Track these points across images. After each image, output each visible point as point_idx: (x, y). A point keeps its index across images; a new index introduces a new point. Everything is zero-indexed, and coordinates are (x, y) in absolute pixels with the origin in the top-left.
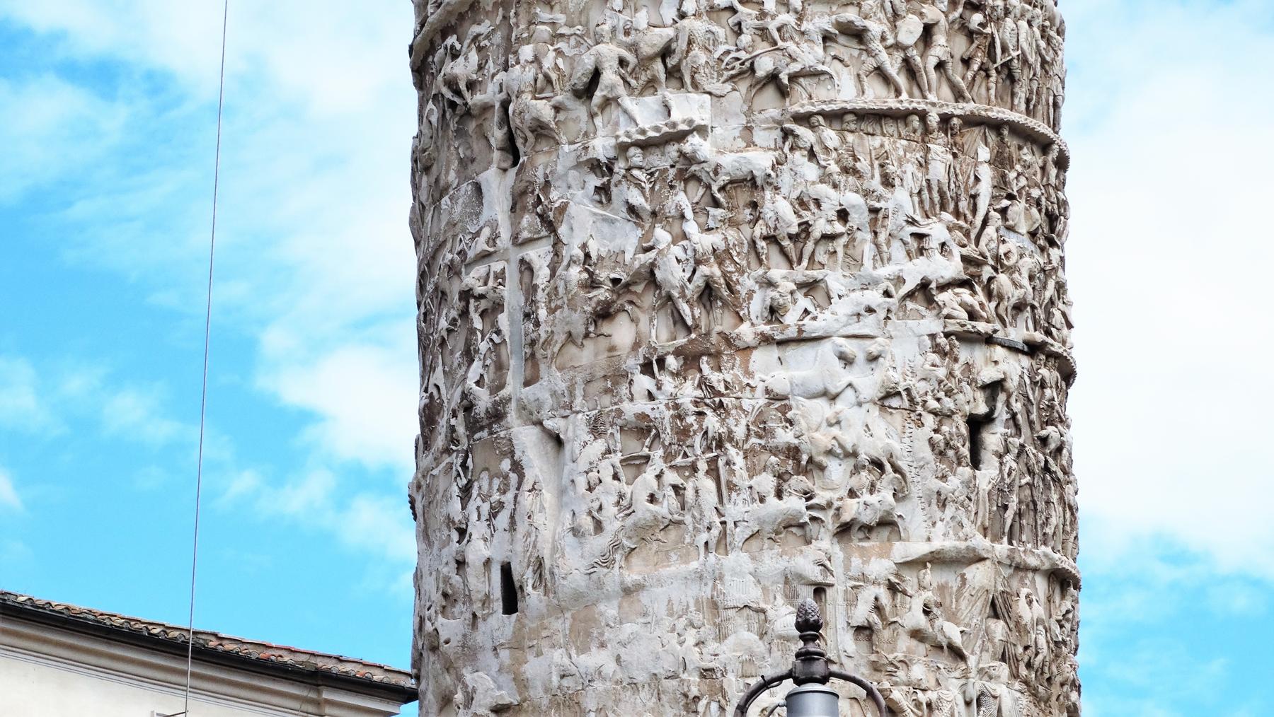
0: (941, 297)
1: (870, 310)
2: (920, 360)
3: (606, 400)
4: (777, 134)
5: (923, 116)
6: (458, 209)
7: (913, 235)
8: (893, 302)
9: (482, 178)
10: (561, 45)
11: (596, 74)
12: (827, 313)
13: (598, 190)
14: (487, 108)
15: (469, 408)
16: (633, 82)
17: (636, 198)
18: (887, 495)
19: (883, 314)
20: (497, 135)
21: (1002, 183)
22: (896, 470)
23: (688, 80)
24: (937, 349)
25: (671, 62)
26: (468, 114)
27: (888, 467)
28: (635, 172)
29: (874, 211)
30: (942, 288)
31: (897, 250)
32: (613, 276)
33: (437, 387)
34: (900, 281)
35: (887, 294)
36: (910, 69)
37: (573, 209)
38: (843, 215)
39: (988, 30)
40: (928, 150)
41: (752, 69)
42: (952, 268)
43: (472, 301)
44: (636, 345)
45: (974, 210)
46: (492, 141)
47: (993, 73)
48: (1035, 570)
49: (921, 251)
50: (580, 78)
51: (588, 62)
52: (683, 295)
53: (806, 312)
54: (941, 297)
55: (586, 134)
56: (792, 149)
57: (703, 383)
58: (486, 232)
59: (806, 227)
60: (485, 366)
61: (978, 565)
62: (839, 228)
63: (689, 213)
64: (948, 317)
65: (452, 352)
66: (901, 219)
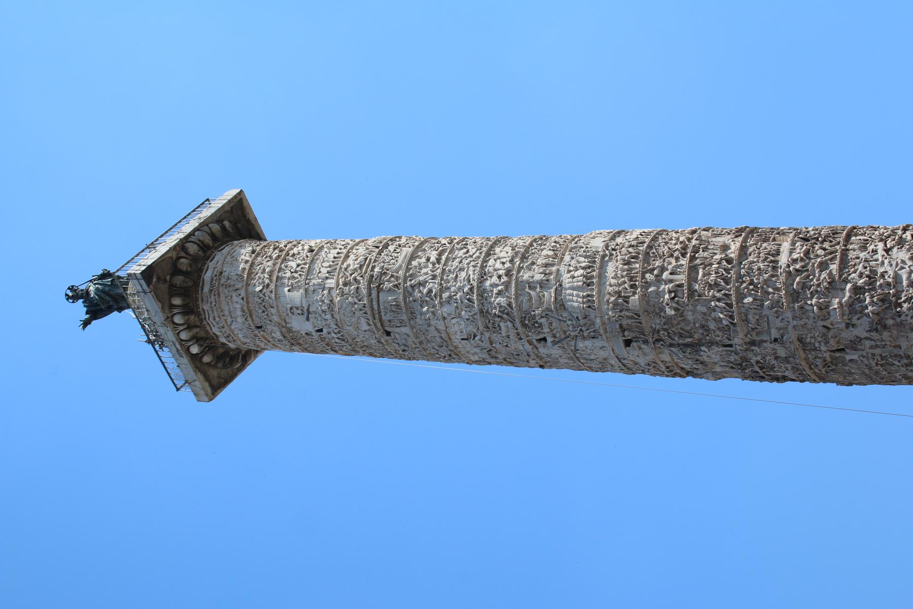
0: (888, 246)
1: (890, 262)
2: (904, 252)
3: (907, 327)
4: (843, 283)
5: (843, 250)
6: (854, 366)
7: (872, 253)
8: (888, 257)
9: (848, 360)
10: (816, 335)
11: (824, 326)
13: (853, 327)
14: (831, 356)
15: (907, 365)
16: (827, 317)
17: (857, 317)
19: (891, 259)
20: (838, 355)
21: (862, 235)
24: (901, 248)
25: (823, 307)
26: (831, 362)
28: (849, 317)
29: (865, 261)
30: (886, 247)
31: (875, 257)
32: (875, 324)
33: (900, 375)
34: (883, 256)
35: (886, 258)
36: (831, 253)
37: (857, 334)
38: (865, 268)
39: (823, 236)
40: (851, 249)
41: (827, 288)
42: (881, 246)
43: (879, 363)
44: (893, 319)
45: (867, 240)
46: (838, 355)
49: (876, 251)
50: (824, 330)
51: (821, 328)
52: (881, 306)
53: (889, 277)
54: (888, 246)
55: (839, 330)
56: (848, 279)
57: (904, 302)
58: (861, 358)
60: (895, 360)
63: (861, 304)
65: (891, 370)
66: (868, 255)
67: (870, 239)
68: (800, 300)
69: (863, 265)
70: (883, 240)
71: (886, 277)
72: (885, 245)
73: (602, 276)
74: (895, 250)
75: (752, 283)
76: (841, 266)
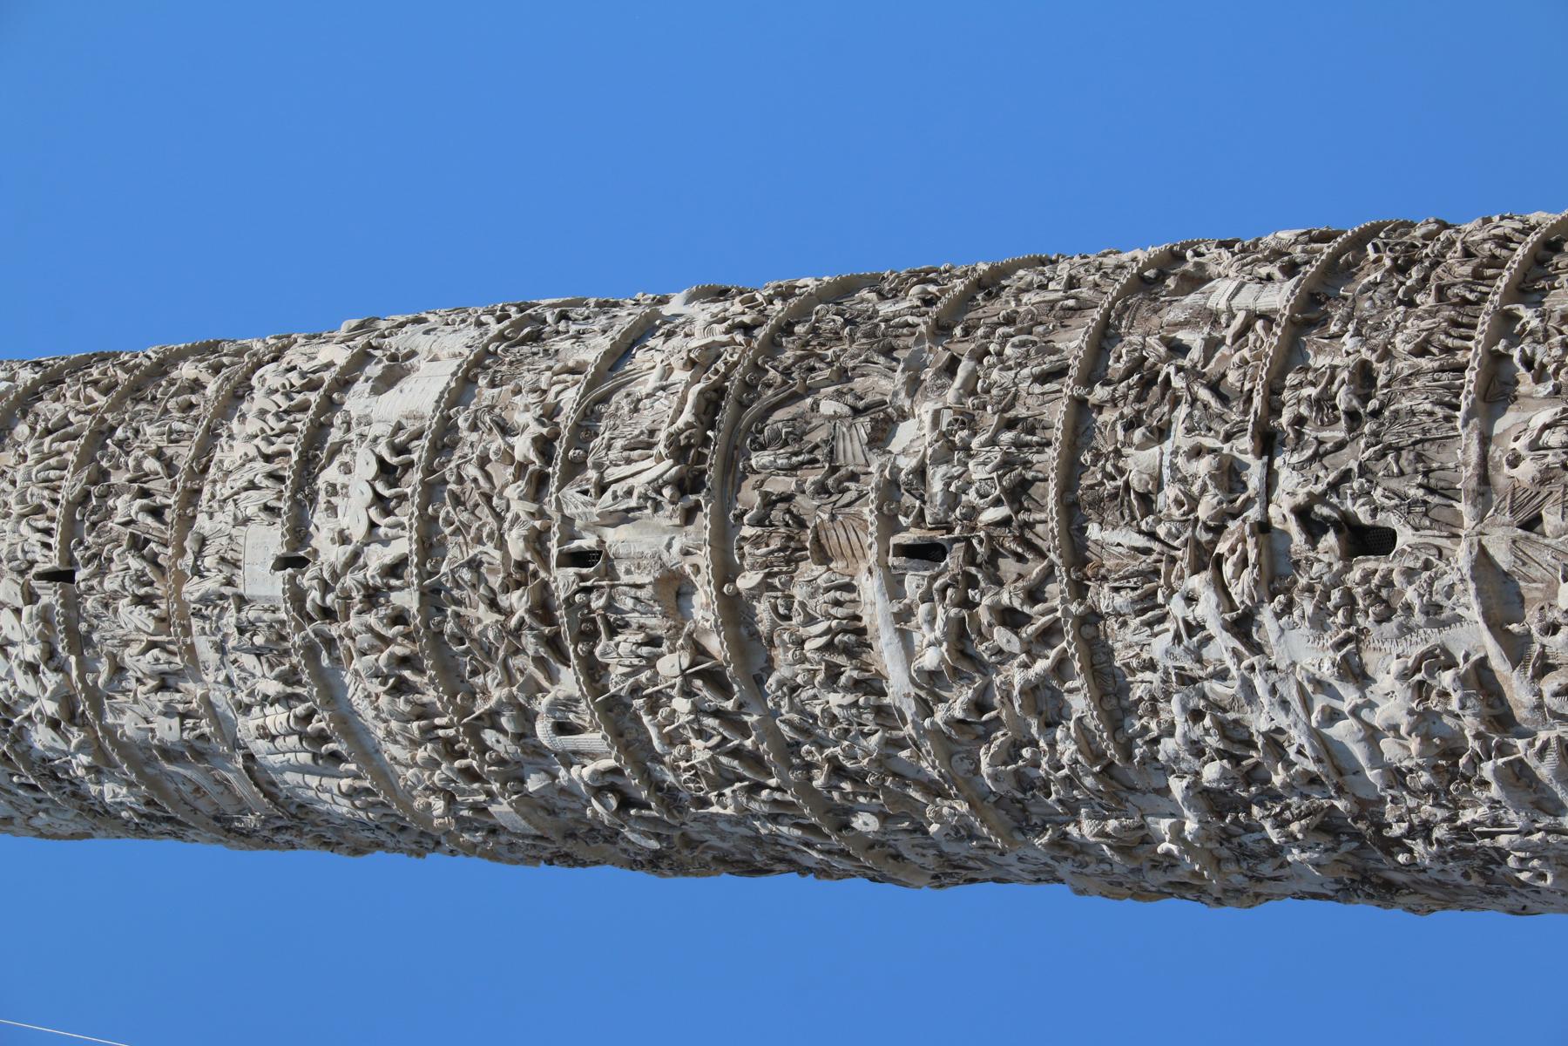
1: (1273, 691)
7: (1190, 636)
12: (1293, 732)
18: (1446, 678)
19: (1273, 676)
22: (1418, 670)
23: (1142, 833)
24: (1288, 607)
27: (1418, 677)
45: (1147, 551)
47: (1022, 516)
48: (1486, 440)
59: (1221, 754)
61: (1491, 551)
62: (1207, 722)
64: (1252, 598)
66: (1179, 650)
67: (1157, 546)
68: (1035, 820)
69: (1184, 707)
70: (1205, 559)
71: (1292, 752)
72: (1222, 588)
73: (347, 723)
74: (1266, 615)
75: (838, 771)
76: (1107, 707)
